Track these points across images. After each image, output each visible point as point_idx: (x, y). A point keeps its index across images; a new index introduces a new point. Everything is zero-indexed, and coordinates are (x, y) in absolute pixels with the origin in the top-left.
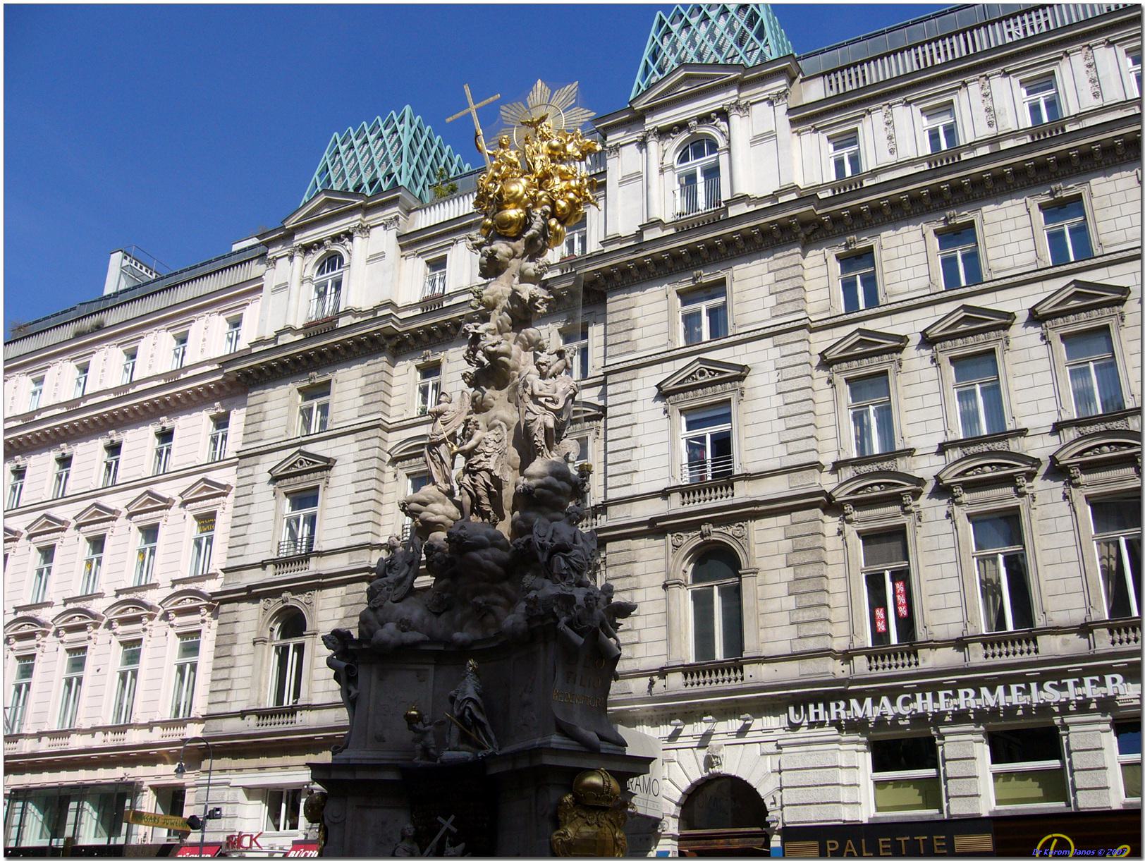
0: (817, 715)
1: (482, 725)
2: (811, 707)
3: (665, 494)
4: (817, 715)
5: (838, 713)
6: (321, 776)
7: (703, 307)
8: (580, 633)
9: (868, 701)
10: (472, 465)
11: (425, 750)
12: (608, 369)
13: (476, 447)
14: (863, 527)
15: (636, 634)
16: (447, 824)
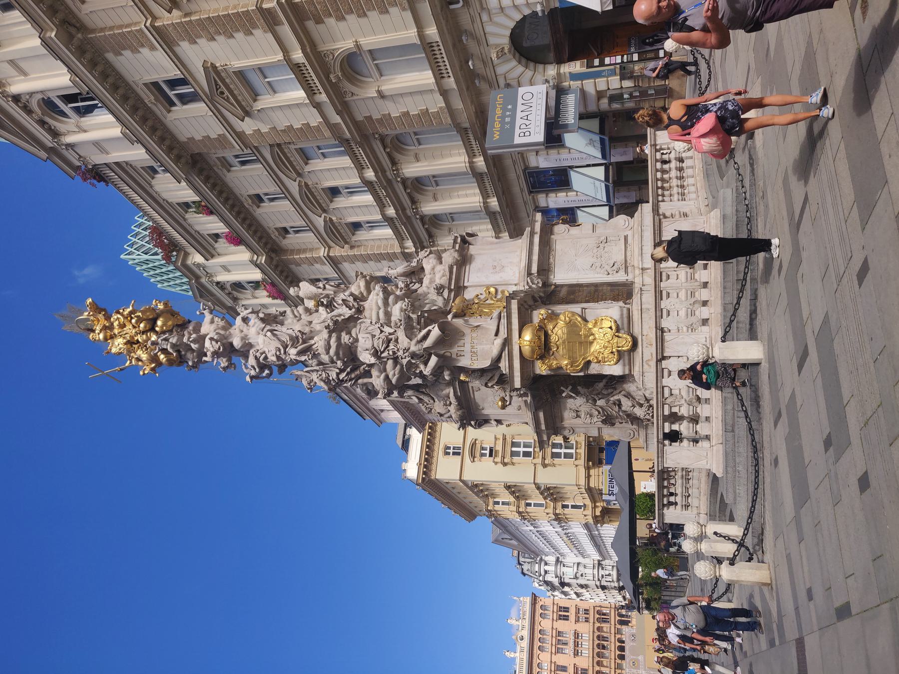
7: (171, 94)
8: (430, 355)
13: (324, 381)
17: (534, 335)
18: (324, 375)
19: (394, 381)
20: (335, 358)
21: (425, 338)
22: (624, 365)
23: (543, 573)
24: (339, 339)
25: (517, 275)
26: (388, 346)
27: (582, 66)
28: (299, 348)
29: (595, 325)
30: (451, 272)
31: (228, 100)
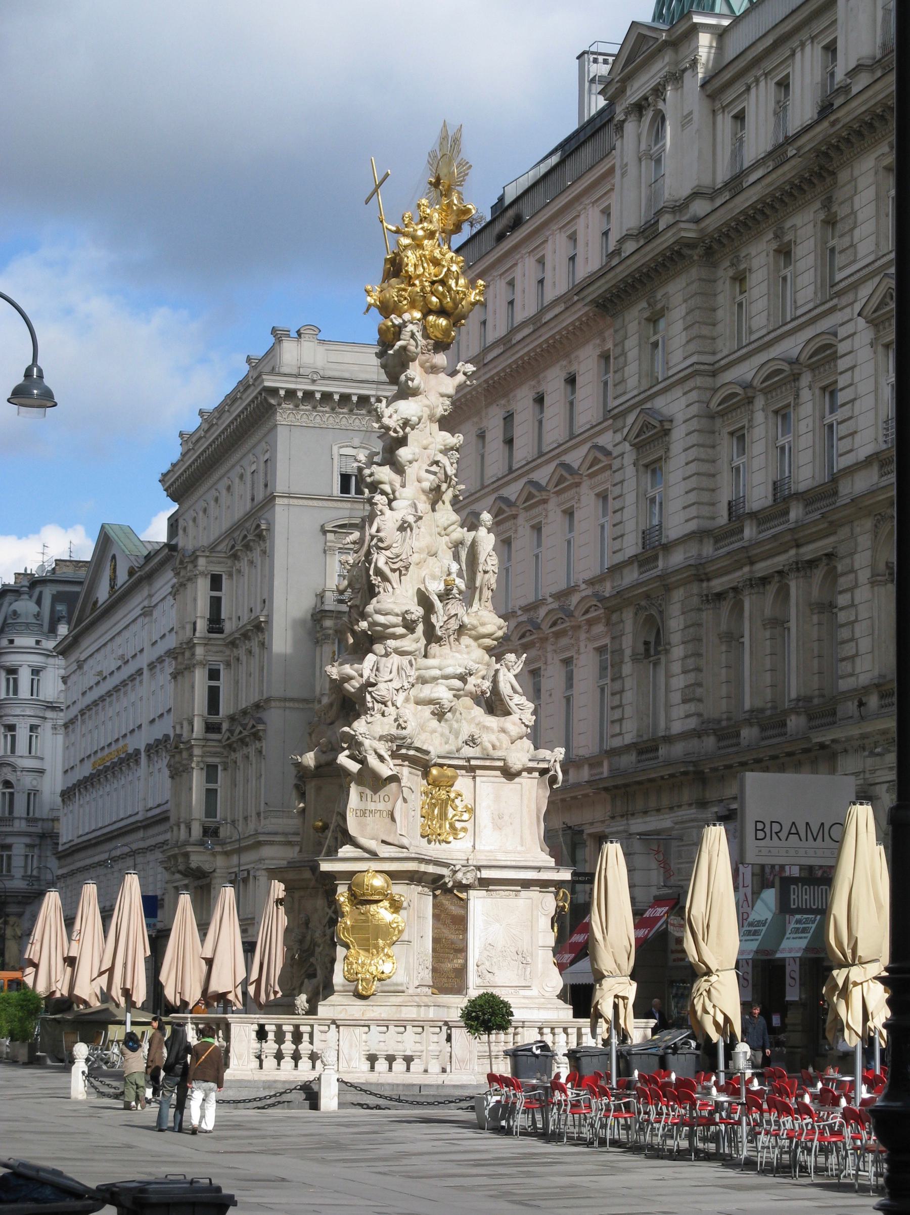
15: (853, 644)
19: (346, 685)
21: (381, 758)
22: (343, 986)
25: (487, 848)
26: (378, 702)
28: (386, 570)
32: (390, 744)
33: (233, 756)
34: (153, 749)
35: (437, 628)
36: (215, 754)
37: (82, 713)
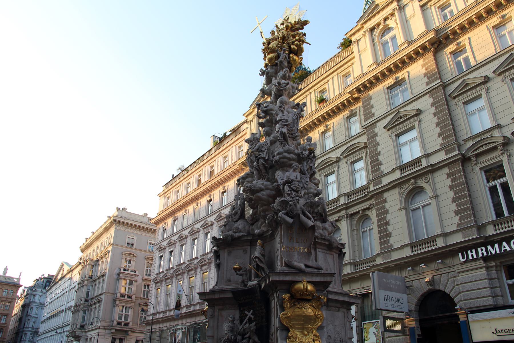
0: (472, 256)
1: (263, 269)
2: (469, 252)
3: (393, 171)
4: (472, 256)
5: (483, 254)
6: (204, 298)
8: (291, 217)
9: (496, 246)
10: (256, 157)
11: (243, 282)
12: (365, 126)
14: (482, 166)
16: (249, 314)
17: (310, 292)
18: (263, 149)
20: (281, 156)
23: (34, 293)
24: (293, 160)
26: (294, 190)
27: (419, 335)
29: (315, 336)
30: (325, 239)
31: (396, 121)
32: (309, 209)
33: (91, 308)
34: (67, 309)
35: (305, 170)
36: (86, 307)
37: (50, 303)
